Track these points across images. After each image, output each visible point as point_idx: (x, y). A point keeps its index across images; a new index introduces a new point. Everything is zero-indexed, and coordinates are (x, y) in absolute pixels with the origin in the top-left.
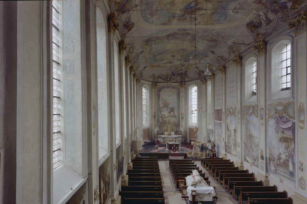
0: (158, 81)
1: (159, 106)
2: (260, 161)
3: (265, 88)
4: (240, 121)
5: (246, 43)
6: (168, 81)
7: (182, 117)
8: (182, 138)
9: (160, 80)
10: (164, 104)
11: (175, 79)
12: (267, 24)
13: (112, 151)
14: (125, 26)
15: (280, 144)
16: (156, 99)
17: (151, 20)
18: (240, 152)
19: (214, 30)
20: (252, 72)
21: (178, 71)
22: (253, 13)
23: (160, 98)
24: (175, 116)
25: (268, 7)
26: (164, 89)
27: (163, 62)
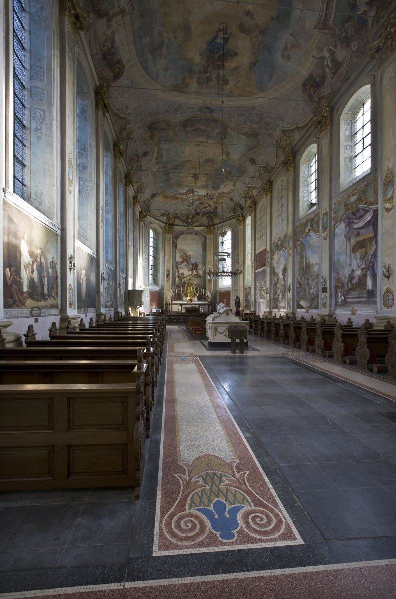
1: (176, 260)
2: (321, 295)
3: (331, 180)
4: (291, 251)
5: (301, 126)
6: (189, 224)
9: (177, 222)
10: (183, 258)
12: (334, 74)
14: (105, 58)
15: (353, 255)
18: (291, 298)
19: (254, 109)
20: (310, 175)
22: (313, 57)
24: (198, 276)
25: (337, 34)
26: (183, 235)
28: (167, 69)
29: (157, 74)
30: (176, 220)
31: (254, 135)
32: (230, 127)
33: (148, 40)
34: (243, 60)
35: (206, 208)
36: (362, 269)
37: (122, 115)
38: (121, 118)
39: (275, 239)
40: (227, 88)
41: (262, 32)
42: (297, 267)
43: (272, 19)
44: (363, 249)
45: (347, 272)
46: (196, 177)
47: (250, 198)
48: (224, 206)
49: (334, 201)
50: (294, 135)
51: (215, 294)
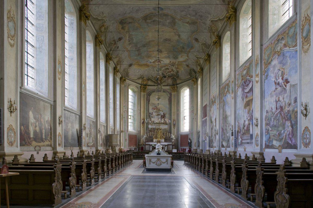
1: (149, 112)
6: (159, 84)
8: (172, 146)
9: (150, 83)
13: (55, 101)
15: (245, 110)
21: (169, 72)
23: (150, 102)
26: (154, 93)
27: (150, 60)
30: (149, 82)
31: (194, 23)
32: (177, 18)
35: (170, 72)
36: (249, 120)
37: (99, 18)
38: (99, 20)
39: (212, 97)
42: (221, 118)
44: (249, 107)
45: (242, 122)
46: (159, 51)
47: (199, 65)
48: (183, 72)
49: (237, 73)
50: (219, 24)
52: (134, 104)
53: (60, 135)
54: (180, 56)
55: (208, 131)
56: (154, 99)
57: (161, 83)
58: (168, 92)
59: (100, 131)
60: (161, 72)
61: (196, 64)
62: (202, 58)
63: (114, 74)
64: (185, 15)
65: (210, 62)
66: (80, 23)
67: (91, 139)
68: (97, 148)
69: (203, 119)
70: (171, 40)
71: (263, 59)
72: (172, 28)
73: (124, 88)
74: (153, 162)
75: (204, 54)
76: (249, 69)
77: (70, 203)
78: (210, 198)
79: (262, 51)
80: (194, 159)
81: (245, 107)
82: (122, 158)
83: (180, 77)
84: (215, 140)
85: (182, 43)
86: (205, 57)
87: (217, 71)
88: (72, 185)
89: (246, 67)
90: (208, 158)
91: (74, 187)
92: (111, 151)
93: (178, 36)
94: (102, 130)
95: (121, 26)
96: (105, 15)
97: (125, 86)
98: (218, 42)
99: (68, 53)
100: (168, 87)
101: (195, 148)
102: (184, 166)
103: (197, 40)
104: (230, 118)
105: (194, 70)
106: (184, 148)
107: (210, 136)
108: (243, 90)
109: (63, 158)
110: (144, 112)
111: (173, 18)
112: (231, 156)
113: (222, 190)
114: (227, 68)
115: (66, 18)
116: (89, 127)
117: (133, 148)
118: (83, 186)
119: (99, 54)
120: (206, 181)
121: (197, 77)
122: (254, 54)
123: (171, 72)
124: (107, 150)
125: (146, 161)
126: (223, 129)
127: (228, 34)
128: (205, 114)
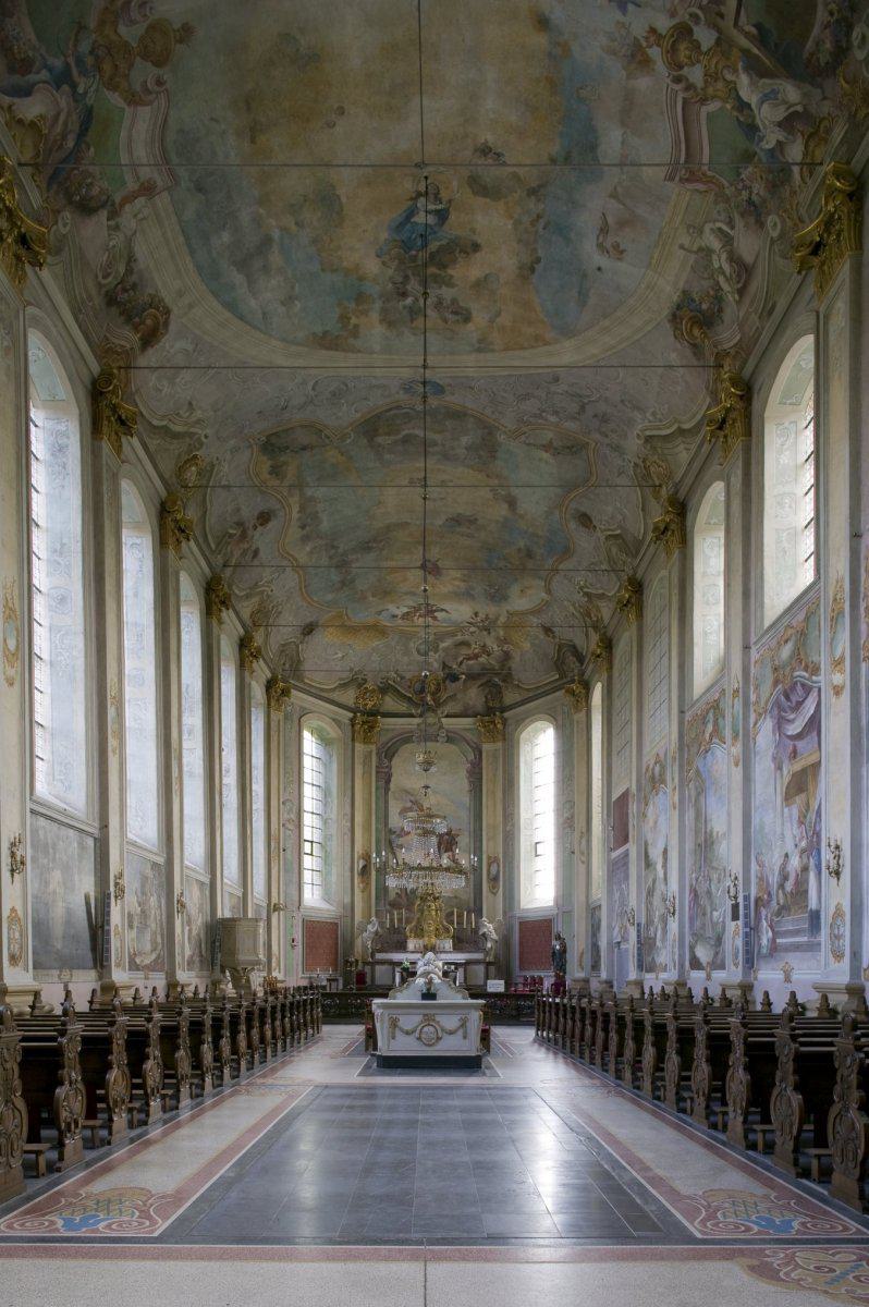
0: (381, 711)
1: (386, 824)
7: (491, 876)
9: (390, 703)
11: (459, 696)
16: (374, 790)
17: (253, 303)
23: (392, 785)
27: (393, 609)
28: (290, 298)
29: (264, 314)
30: (387, 698)
31: (571, 448)
33: (225, 239)
34: (500, 257)
35: (476, 657)
40: (471, 330)
41: (533, 192)
43: (553, 161)
46: (430, 569)
47: (595, 628)
48: (528, 657)
51: (510, 929)
52: (325, 792)
53: (14, 918)
54: (515, 590)
55: (633, 902)
56: (407, 773)
57: (439, 705)
58: (466, 741)
59: (183, 906)
60: (437, 656)
61: (585, 622)
62: (610, 599)
63: (242, 666)
64: (535, 416)
65: (640, 615)
66: (93, 445)
67: (148, 937)
68: (171, 974)
69: (614, 855)
70: (476, 519)
71: (862, 596)
72: (481, 471)
73: (281, 723)
74: (408, 1027)
75: (615, 579)
76: (803, 636)
77: (61, 1194)
78: (645, 1169)
79: (859, 559)
80: (578, 1016)
81: (786, 799)
82: (279, 1016)
83: (516, 678)
84: (664, 939)
85: (526, 532)
86: (618, 591)
87: (670, 650)
88: (69, 1120)
89: (790, 632)
90: (633, 1011)
91: (77, 1127)
92: (229, 989)
93: (506, 506)
94: (194, 899)
95: (269, 463)
96: (198, 414)
97: (286, 718)
98: (673, 526)
99: (47, 575)
100: (466, 722)
101: (582, 975)
102: (536, 1046)
103: (585, 520)
104: (724, 845)
105: (574, 647)
106: (536, 974)
107: (643, 921)
108: (779, 728)
109: (32, 1013)
110: (367, 827)
111: (485, 427)
112: (731, 1002)
113: (691, 1137)
114: (713, 638)
115: (36, 426)
116: (136, 885)
117: (322, 976)
118: (115, 1126)
119: (178, 580)
120: (628, 1106)
121: (586, 677)
122: (826, 572)
123: (481, 659)
124: (215, 984)
125: (378, 1025)
126: (695, 894)
127: (716, 491)
128: (620, 831)
